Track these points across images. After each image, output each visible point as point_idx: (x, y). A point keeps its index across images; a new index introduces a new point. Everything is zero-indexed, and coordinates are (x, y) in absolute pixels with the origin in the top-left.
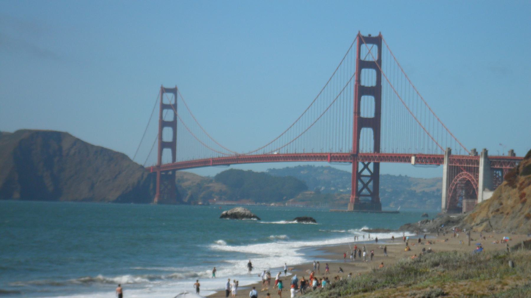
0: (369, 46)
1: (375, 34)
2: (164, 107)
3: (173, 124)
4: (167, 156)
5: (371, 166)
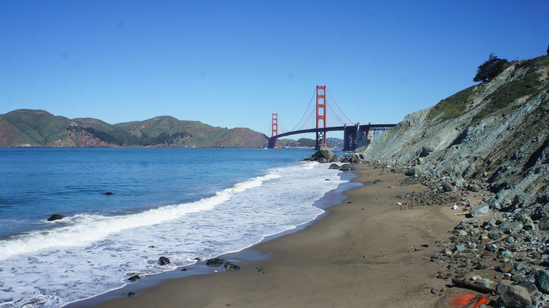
0: (321, 90)
1: (323, 86)
2: (273, 119)
3: (276, 124)
4: (275, 134)
5: (323, 133)
